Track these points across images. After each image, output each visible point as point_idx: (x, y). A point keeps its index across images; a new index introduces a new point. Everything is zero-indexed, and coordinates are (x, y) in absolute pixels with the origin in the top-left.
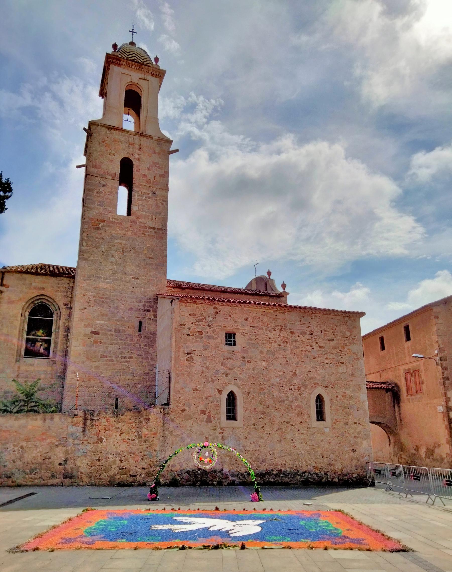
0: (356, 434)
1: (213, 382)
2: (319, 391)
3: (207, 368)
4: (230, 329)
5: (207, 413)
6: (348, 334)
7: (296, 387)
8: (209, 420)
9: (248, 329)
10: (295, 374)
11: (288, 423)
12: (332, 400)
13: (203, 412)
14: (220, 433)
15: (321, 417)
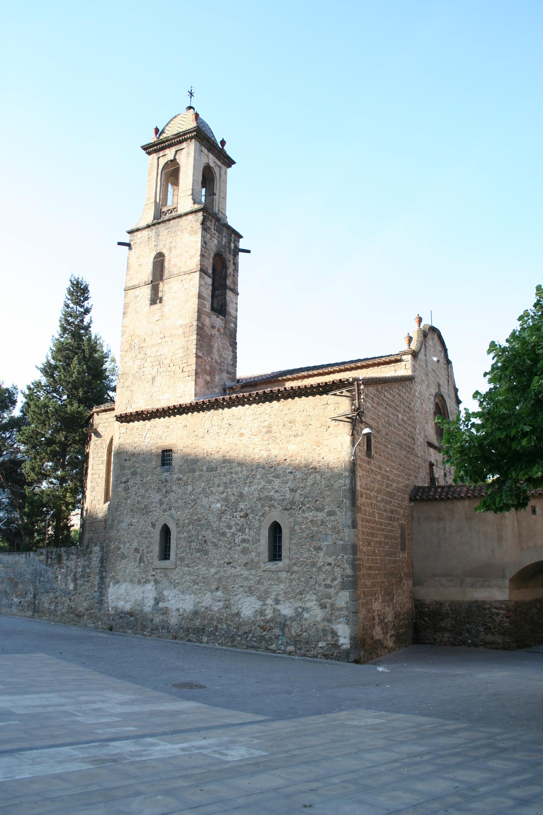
0: (328, 582)
1: (147, 513)
2: (276, 515)
3: (143, 497)
5: (140, 551)
7: (242, 514)
11: (229, 563)
14: (152, 575)
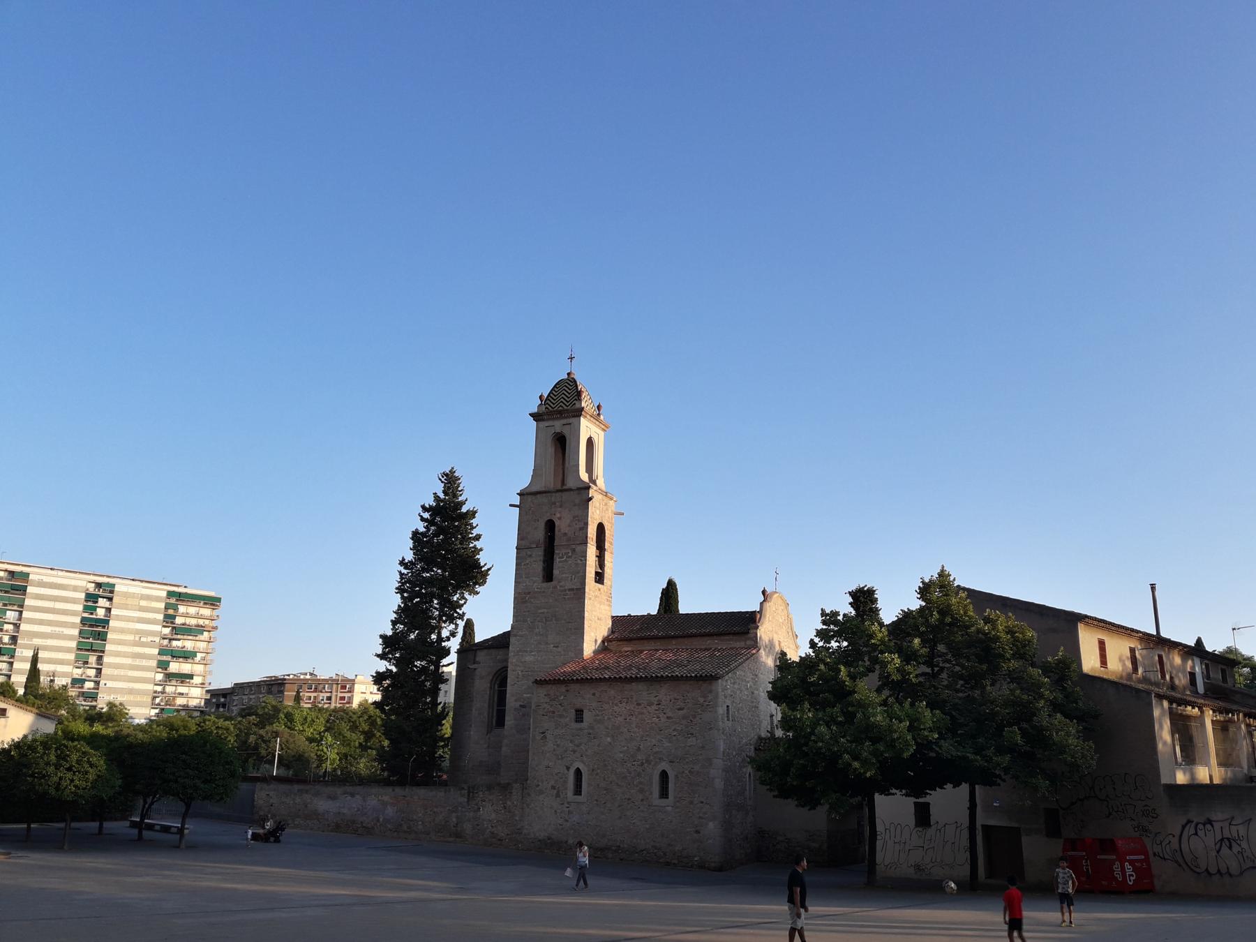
2: (664, 766)
4: (578, 706)
6: (701, 700)
8: (558, 795)
9: (594, 704)
10: (639, 749)
12: (676, 776)
13: (553, 788)
15: (664, 793)
